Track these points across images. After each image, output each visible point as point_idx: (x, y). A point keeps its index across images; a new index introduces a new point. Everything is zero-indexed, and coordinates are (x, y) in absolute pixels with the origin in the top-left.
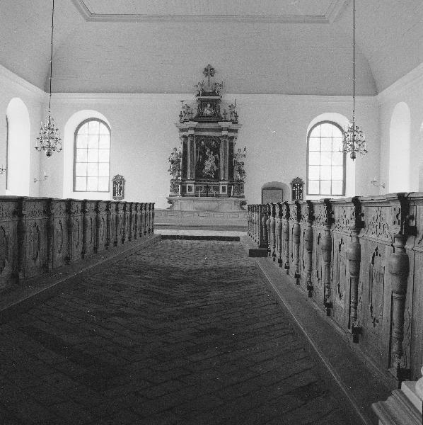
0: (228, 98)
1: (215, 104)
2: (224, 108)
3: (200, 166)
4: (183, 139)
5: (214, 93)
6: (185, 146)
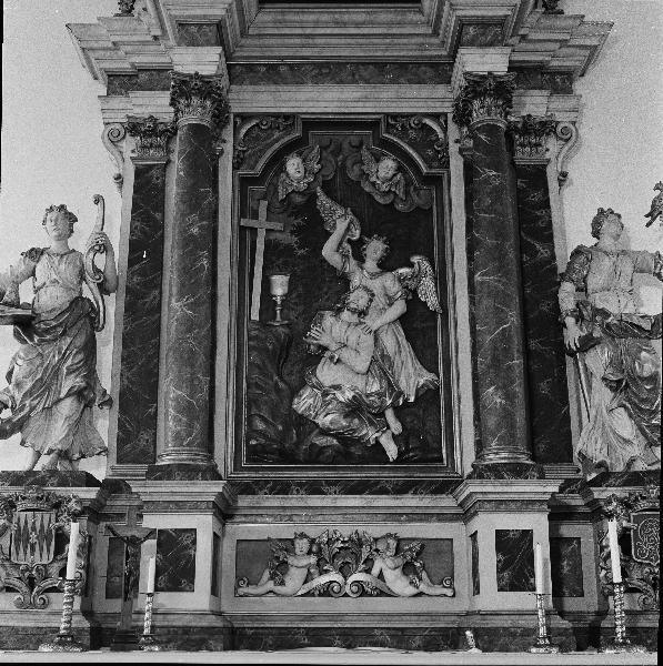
3: (285, 355)
4: (130, 145)
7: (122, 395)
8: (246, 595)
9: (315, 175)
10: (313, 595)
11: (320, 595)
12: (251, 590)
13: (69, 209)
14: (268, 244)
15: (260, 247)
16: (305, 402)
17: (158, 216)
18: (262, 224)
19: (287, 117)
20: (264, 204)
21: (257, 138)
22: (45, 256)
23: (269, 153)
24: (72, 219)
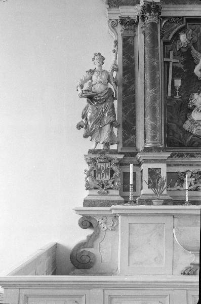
4: (119, 28)
6: (128, 49)
7: (123, 123)
8: (170, 191)
9: (190, 41)
10: (192, 190)
11: (194, 190)
12: (172, 189)
13: (102, 55)
14: (173, 67)
15: (171, 69)
16: (187, 126)
17: (132, 57)
18: (171, 60)
19: (179, 17)
20: (171, 53)
21: (168, 26)
22: (96, 73)
23: (174, 32)
24: (103, 58)
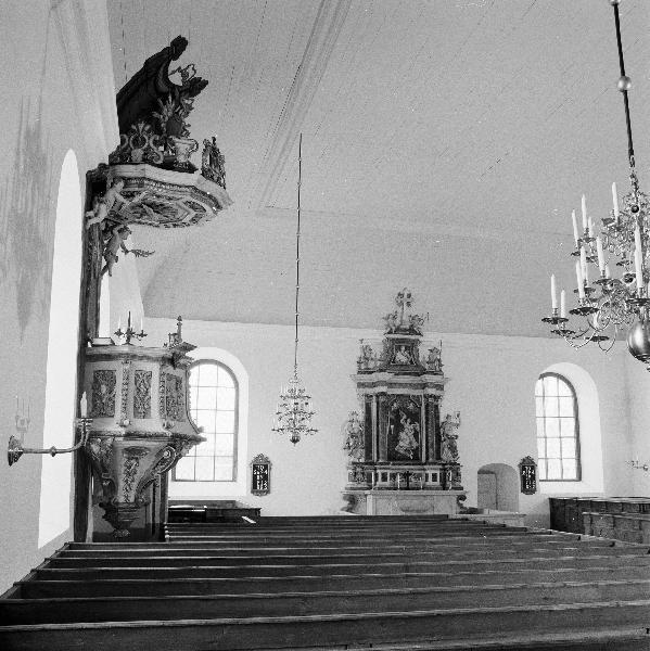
0: (428, 341)
1: (411, 347)
2: (423, 353)
3: (394, 439)
5: (412, 331)
